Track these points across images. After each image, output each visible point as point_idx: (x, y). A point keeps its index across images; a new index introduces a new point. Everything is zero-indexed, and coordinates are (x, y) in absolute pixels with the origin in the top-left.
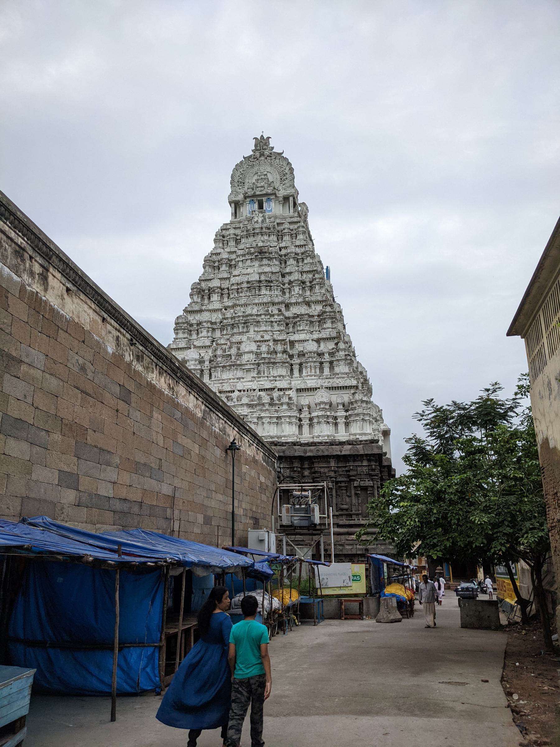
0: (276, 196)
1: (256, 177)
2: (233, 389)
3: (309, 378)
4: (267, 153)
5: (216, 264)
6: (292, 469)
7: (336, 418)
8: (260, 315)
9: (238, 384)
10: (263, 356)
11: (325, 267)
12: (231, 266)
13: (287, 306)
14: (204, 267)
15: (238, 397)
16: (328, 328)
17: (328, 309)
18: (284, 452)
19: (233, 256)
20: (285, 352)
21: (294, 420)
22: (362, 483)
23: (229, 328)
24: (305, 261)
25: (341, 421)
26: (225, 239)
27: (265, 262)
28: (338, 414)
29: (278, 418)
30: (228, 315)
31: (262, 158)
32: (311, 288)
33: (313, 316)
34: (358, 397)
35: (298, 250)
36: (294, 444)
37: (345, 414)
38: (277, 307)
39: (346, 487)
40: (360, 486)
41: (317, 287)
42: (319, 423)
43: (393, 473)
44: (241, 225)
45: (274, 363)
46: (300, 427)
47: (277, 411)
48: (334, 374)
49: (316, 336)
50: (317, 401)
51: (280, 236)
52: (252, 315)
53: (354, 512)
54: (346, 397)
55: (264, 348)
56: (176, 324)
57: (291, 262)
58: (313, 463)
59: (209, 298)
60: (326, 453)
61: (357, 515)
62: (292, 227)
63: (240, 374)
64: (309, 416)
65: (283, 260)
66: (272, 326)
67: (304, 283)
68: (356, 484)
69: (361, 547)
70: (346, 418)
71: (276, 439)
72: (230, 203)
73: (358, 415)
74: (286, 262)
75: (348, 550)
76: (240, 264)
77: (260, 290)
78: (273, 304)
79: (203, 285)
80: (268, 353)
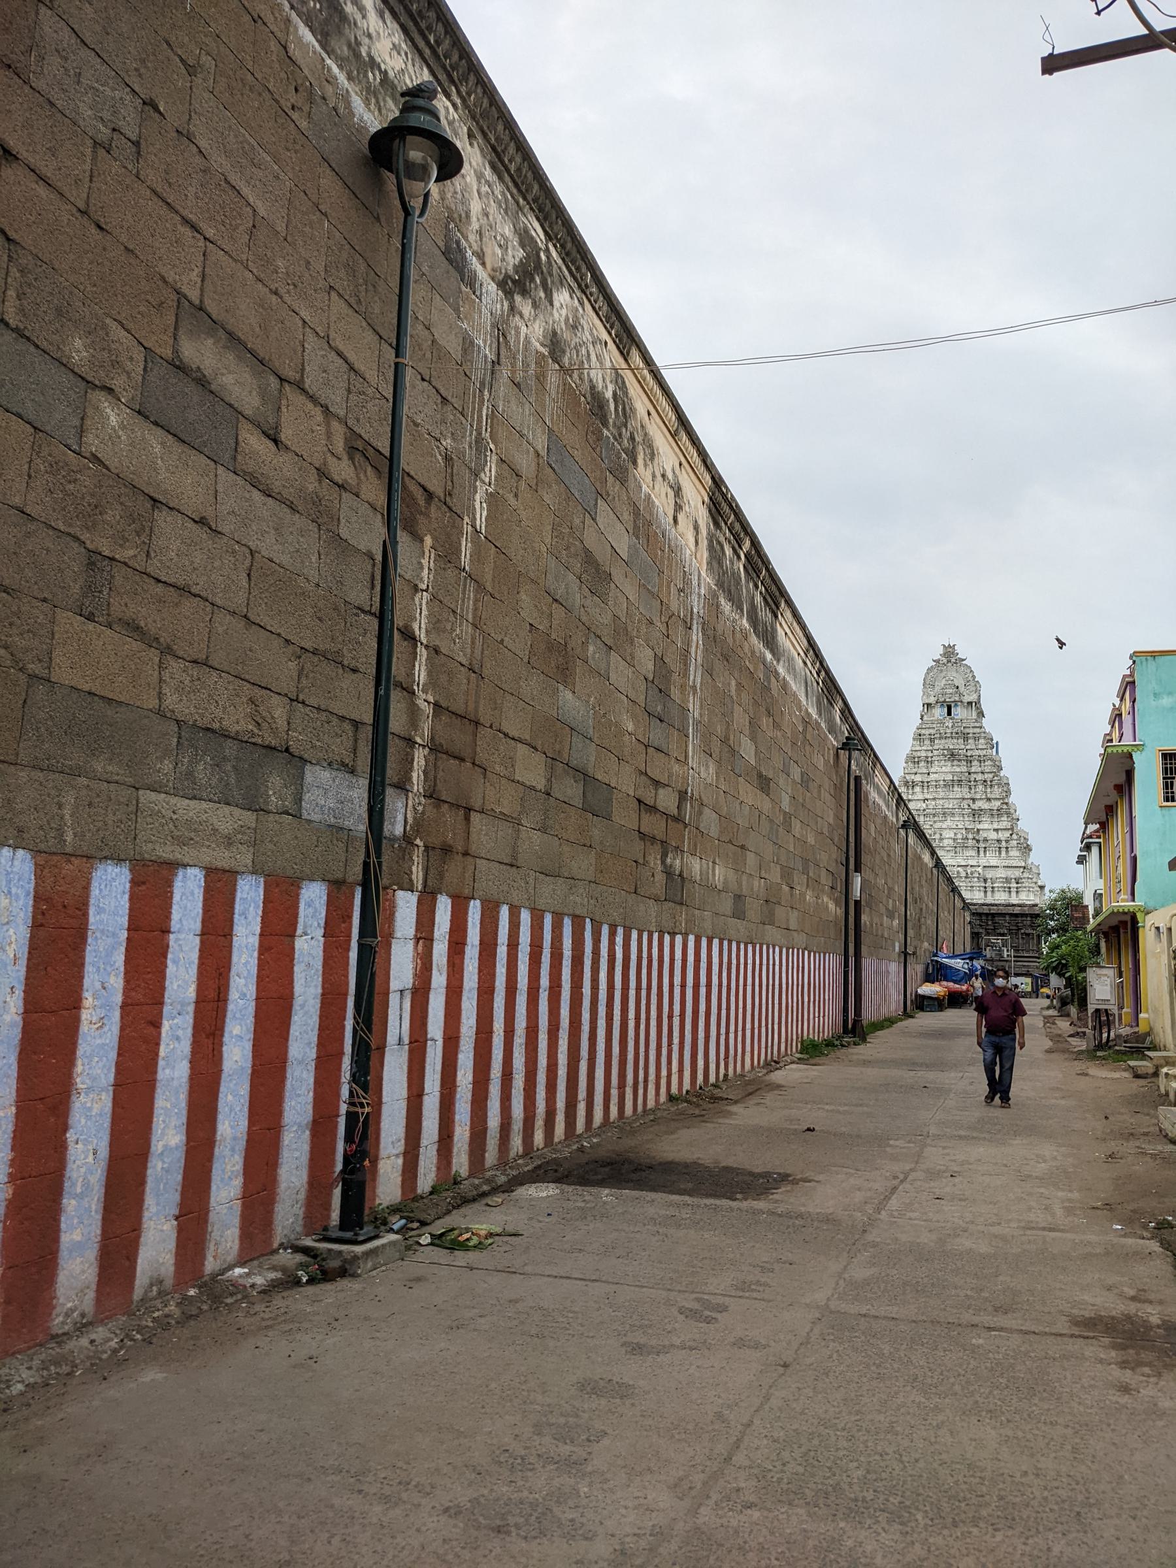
1: (944, 682)
6: (981, 920)
12: (929, 762)
19: (930, 754)
27: (956, 763)
34: (1026, 875)
35: (982, 753)
46: (985, 892)
49: (996, 826)
51: (966, 739)
54: (1017, 873)
55: (959, 836)
65: (969, 761)
79: (908, 777)
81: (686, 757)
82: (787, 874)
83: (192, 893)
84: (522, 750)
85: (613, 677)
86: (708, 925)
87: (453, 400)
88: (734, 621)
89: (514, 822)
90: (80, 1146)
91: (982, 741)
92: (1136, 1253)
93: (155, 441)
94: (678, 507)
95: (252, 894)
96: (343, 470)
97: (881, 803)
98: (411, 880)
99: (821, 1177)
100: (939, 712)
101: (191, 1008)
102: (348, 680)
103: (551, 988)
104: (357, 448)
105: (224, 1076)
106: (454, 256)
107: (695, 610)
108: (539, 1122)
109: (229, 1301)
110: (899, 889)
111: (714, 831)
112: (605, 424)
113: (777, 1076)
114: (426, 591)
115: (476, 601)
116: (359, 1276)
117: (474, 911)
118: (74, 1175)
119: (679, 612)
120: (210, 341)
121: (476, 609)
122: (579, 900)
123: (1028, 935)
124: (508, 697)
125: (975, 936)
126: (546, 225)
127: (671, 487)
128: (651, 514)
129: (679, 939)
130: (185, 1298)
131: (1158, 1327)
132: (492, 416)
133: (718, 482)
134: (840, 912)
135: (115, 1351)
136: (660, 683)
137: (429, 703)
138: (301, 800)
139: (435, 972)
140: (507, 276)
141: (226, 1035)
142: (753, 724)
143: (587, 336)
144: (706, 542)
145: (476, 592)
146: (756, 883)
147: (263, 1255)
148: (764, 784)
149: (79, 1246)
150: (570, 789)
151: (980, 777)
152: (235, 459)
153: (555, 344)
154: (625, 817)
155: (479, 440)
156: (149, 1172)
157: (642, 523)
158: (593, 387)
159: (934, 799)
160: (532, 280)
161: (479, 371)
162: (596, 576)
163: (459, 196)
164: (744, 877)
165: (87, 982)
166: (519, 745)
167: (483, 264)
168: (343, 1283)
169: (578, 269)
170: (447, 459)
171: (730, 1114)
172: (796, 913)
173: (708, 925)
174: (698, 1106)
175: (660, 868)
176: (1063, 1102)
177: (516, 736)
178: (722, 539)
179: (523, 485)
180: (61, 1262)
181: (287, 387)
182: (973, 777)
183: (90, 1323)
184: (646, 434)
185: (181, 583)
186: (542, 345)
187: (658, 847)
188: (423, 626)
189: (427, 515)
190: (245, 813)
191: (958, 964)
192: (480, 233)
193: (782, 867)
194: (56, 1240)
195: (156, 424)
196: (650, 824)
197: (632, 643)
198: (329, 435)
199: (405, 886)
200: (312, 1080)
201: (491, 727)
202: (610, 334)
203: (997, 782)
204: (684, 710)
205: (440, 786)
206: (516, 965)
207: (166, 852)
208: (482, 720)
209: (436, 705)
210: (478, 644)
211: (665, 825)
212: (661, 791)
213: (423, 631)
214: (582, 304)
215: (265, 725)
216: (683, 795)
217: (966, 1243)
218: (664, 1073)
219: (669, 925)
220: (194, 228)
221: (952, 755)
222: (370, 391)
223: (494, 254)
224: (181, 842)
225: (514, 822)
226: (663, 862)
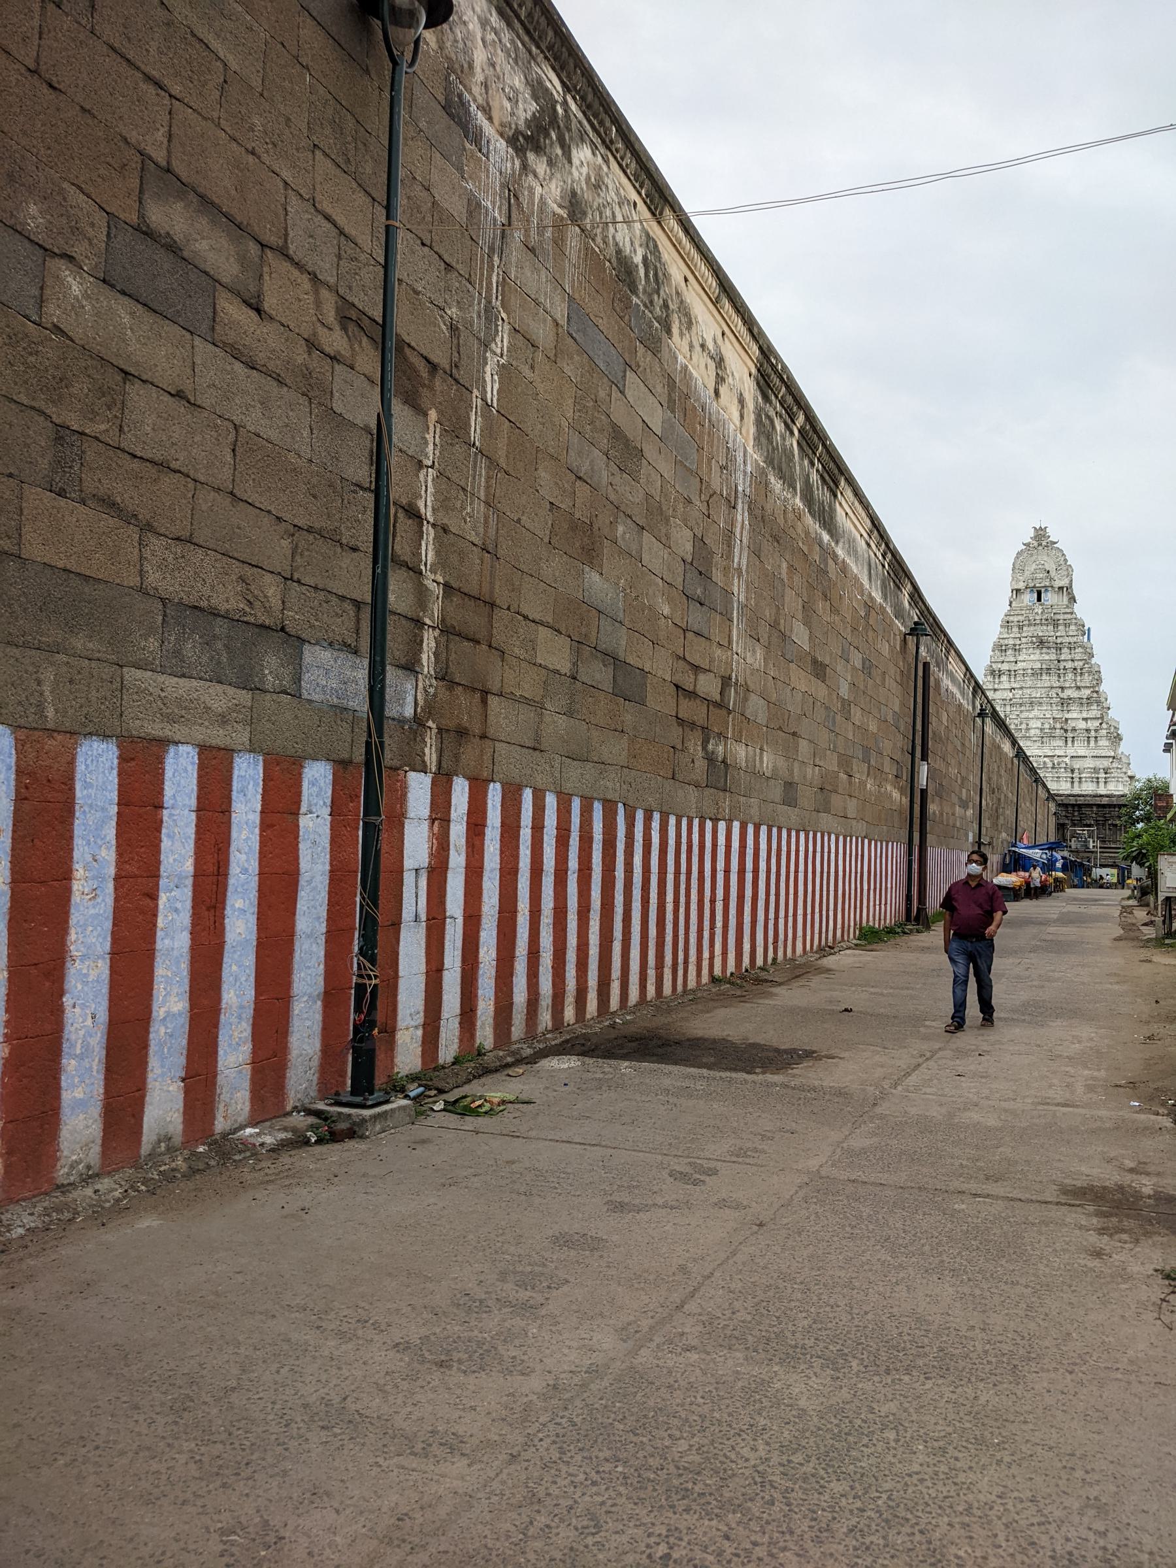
1: (1034, 566)
4: (1044, 543)
6: (1067, 811)
12: (1017, 650)
17: (1095, 695)
19: (1018, 642)
25: (1102, 780)
27: (1044, 650)
34: (1114, 765)
35: (1072, 640)
49: (1085, 715)
51: (1056, 624)
54: (1106, 763)
55: (1046, 726)
62: (1066, 616)
63: (1029, 743)
79: (994, 666)
81: (730, 642)
82: (845, 762)
83: (186, 770)
84: (543, 632)
85: (646, 557)
86: (754, 812)
87: (459, 267)
88: (786, 500)
89: (538, 706)
90: (77, 1010)
91: (1073, 627)
92: (1146, 1128)
93: (123, 312)
94: (720, 379)
95: (251, 772)
96: (335, 341)
97: (955, 690)
98: (424, 762)
99: (846, 1055)
100: (1028, 598)
101: (189, 882)
102: (347, 561)
103: (580, 870)
104: (349, 317)
105: (227, 947)
106: (455, 111)
107: (740, 489)
108: (570, 999)
109: (237, 1157)
110: (973, 779)
111: (762, 718)
112: (634, 291)
113: (830, 961)
114: (432, 467)
115: (488, 478)
116: (368, 1137)
117: (494, 794)
118: (73, 1037)
119: (722, 490)
120: (179, 206)
121: (488, 487)
122: (611, 785)
123: (1116, 825)
124: (527, 578)
125: (1061, 827)
126: (564, 75)
127: (712, 358)
128: (688, 386)
129: (722, 825)
130: (194, 1154)
131: (1149, 1197)
132: (503, 283)
133: (767, 352)
134: (906, 801)
135: (118, 1200)
136: (700, 565)
137: (438, 583)
138: (300, 680)
139: (452, 852)
140: (518, 132)
141: (228, 908)
142: (808, 609)
143: (612, 196)
144: (752, 417)
145: (489, 468)
146: (809, 771)
147: (275, 1117)
148: (819, 670)
149: (80, 1104)
150: (599, 674)
151: (1069, 665)
152: (213, 329)
153: (575, 205)
154: (661, 702)
155: (489, 308)
156: (151, 1036)
157: (678, 396)
158: (619, 252)
159: (1021, 688)
160: (547, 135)
161: (487, 235)
162: (625, 451)
163: (461, 45)
164: (796, 764)
165: (76, 854)
166: (541, 628)
167: (490, 119)
168: (350, 1144)
169: (601, 123)
170: (453, 328)
171: (772, 995)
172: (855, 801)
173: (754, 812)
174: (741, 987)
175: (700, 754)
176: (1116, 987)
177: (537, 617)
178: (772, 413)
179: (540, 356)
180: (64, 1118)
181: (268, 251)
182: (1062, 665)
183: (97, 1175)
184: (682, 302)
185: (158, 457)
186: (560, 206)
187: (698, 733)
188: (429, 503)
189: (431, 388)
190: (238, 691)
191: (1036, 854)
192: (486, 85)
193: (840, 755)
194: (58, 1097)
195: (123, 293)
196: (688, 709)
197: (668, 520)
198: (318, 304)
199: (418, 767)
200: (322, 953)
201: (508, 609)
202: (639, 194)
204: (727, 593)
205: (452, 668)
206: (542, 847)
207: (155, 729)
208: (498, 602)
209: (447, 586)
210: (492, 522)
211: (705, 712)
212: (702, 677)
213: (429, 509)
214: (607, 161)
215: (257, 604)
216: (726, 681)
217: (975, 1116)
218: (706, 955)
219: (712, 811)
220: (159, 85)
221: (1041, 642)
222: (363, 257)
223: (502, 107)
224: (171, 719)
225: (538, 706)
226: (704, 748)
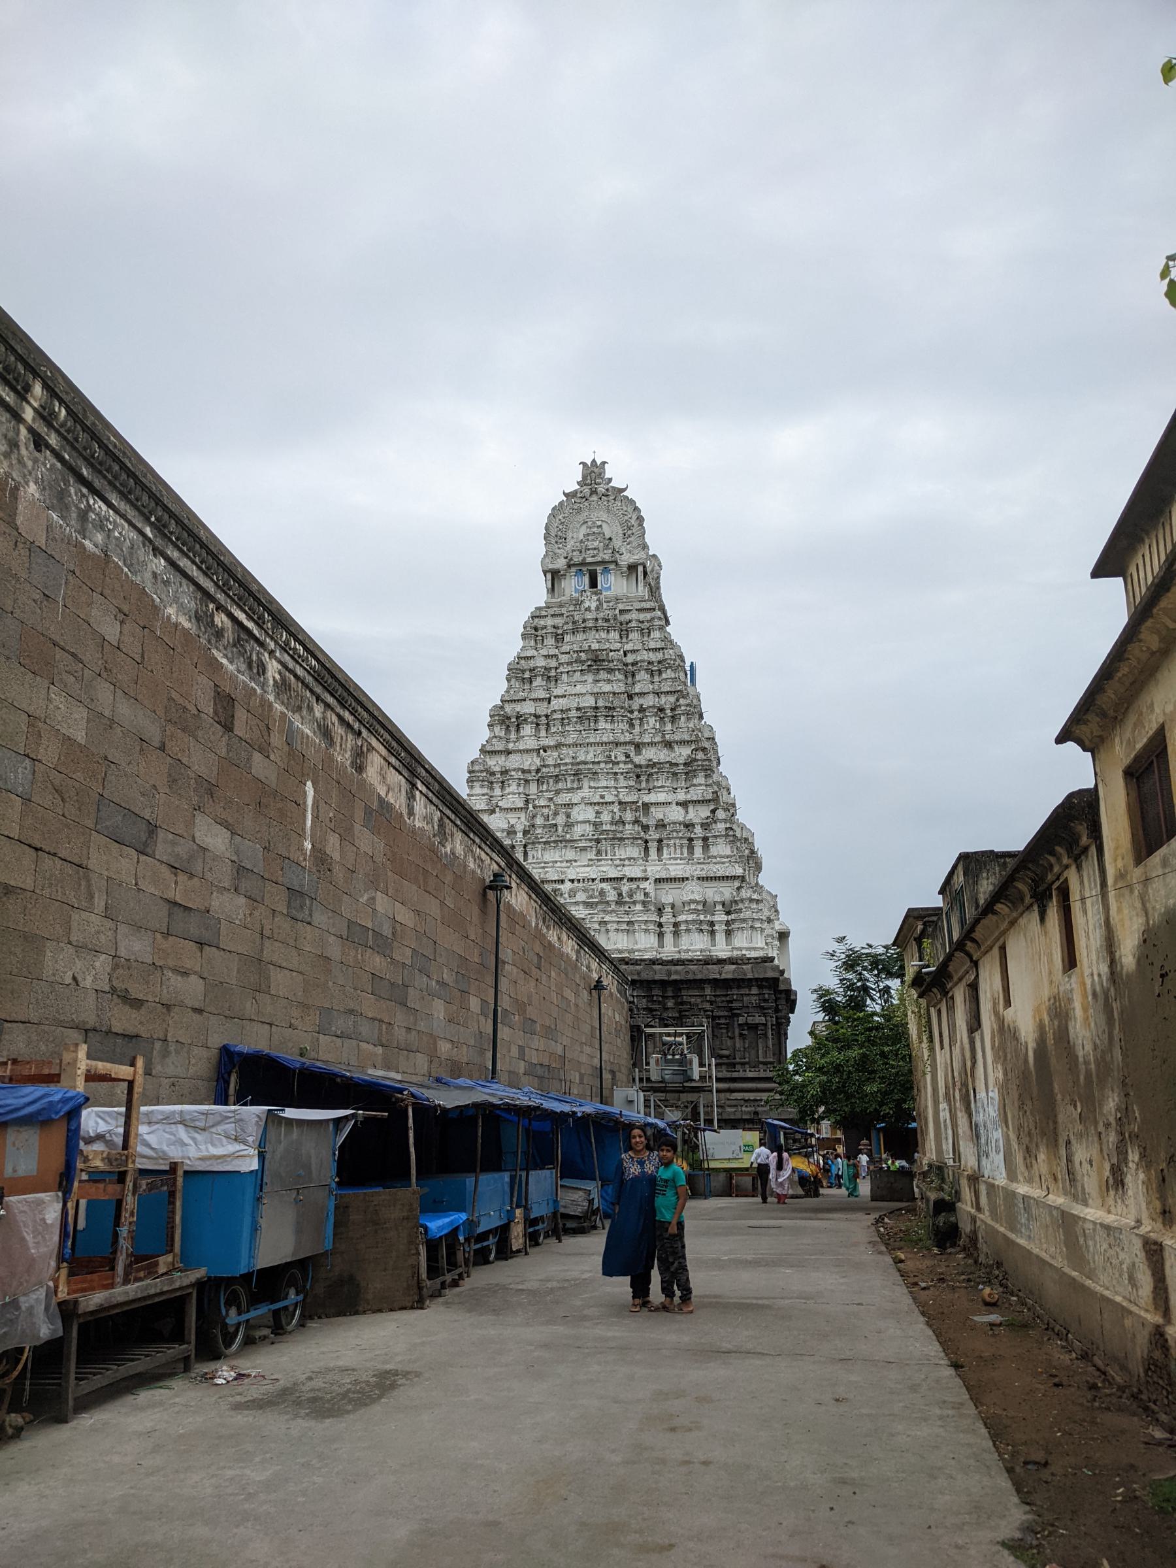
0: (617, 564)
1: (584, 530)
2: (563, 877)
3: (672, 861)
4: (601, 489)
5: (527, 675)
6: (650, 998)
7: (712, 924)
8: (599, 763)
9: (569, 871)
10: (604, 827)
11: (688, 664)
12: (551, 677)
13: (638, 747)
14: (509, 680)
15: (571, 890)
16: (700, 785)
17: (700, 755)
18: (639, 974)
19: (553, 663)
20: (636, 821)
21: (652, 927)
22: (750, 1020)
23: (551, 781)
24: (664, 676)
25: (720, 928)
26: (539, 633)
27: (603, 675)
28: (716, 918)
29: (629, 923)
30: (550, 761)
31: (594, 498)
32: (674, 719)
33: (677, 765)
34: (744, 894)
35: (653, 657)
36: (653, 962)
37: (725, 918)
38: (621, 749)
39: (727, 1024)
40: (747, 1024)
41: (683, 718)
42: (688, 931)
43: (793, 997)
44: (564, 610)
45: (621, 839)
46: (661, 935)
47: (627, 913)
48: (708, 858)
49: (681, 796)
50: (686, 899)
51: (624, 632)
52: (586, 763)
53: (738, 1060)
54: (726, 892)
55: (606, 817)
56: (470, 772)
57: (642, 675)
58: (680, 990)
59: (518, 730)
60: (699, 977)
61: (743, 1064)
62: (642, 616)
63: (570, 854)
64: (673, 920)
65: (630, 672)
66: (616, 780)
67: (661, 710)
68: (741, 1020)
69: (749, 1109)
70: (728, 923)
71: (626, 955)
72: (545, 573)
73: (744, 920)
74: (633, 675)
75: (730, 1113)
76: (565, 677)
77: (596, 722)
78: (617, 744)
79: (508, 708)
80: (612, 823)
91: (656, 634)
100: (572, 585)
123: (754, 1027)
125: (636, 1034)
151: (649, 701)
159: (558, 746)
203: (683, 705)
221: (596, 660)
